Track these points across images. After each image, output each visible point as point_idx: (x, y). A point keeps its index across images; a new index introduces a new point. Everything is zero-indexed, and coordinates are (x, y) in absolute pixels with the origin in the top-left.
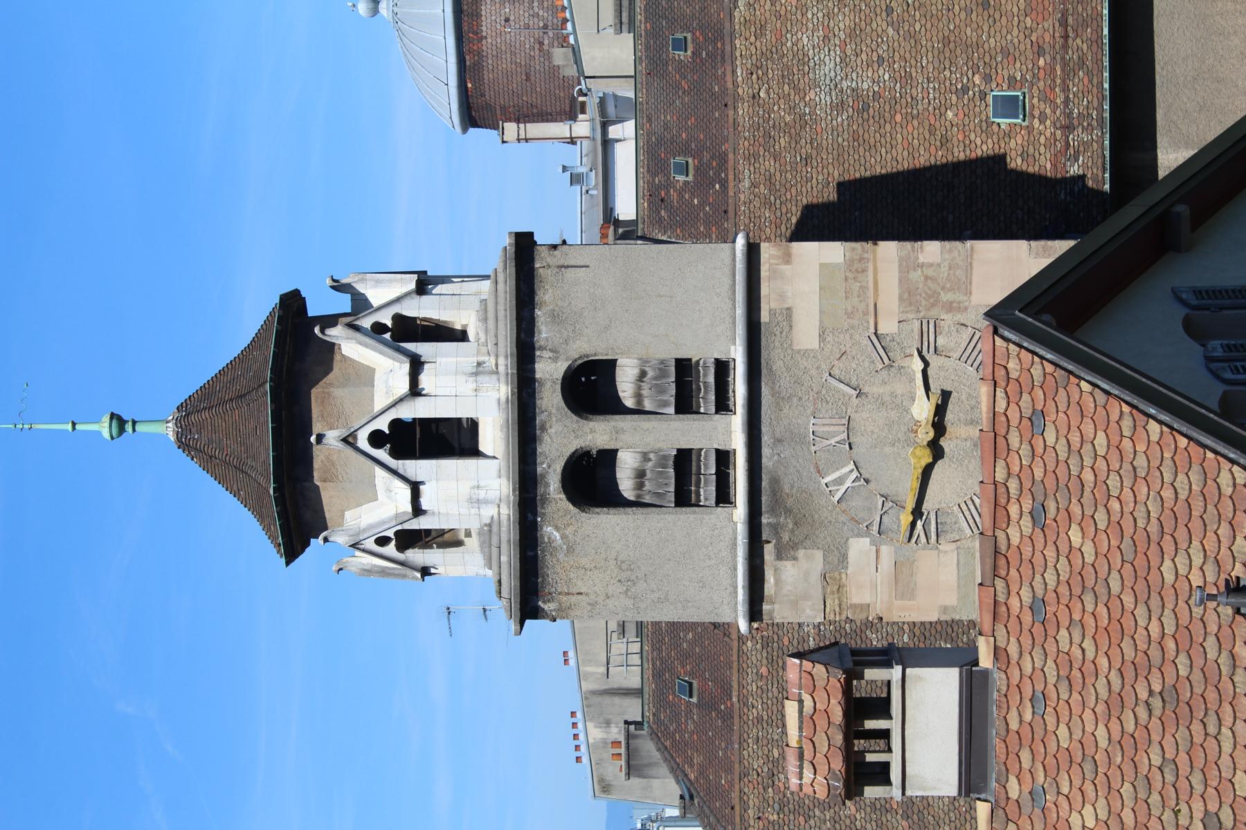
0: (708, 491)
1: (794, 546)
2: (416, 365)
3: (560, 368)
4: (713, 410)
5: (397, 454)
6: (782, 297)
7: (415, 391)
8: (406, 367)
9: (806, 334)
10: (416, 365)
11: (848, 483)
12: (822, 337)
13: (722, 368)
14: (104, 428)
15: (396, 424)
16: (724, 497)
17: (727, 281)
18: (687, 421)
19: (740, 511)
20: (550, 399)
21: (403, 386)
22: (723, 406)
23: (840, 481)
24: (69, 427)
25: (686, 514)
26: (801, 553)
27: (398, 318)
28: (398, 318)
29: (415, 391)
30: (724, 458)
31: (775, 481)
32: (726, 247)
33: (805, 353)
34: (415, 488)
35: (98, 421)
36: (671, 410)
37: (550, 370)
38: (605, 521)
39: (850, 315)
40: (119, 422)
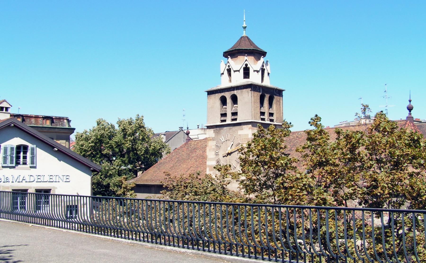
0: (223, 118)
1: (215, 133)
2: (239, 71)
3: (235, 94)
4: (232, 118)
5: (227, 70)
6: (245, 128)
7: (235, 71)
8: (238, 69)
9: (240, 132)
10: (239, 71)
11: (222, 140)
12: (240, 135)
13: (236, 119)
14: (245, 25)
15: (230, 69)
16: (222, 121)
17: (246, 119)
18: (230, 114)
19: (219, 123)
20: (232, 93)
21: (235, 70)
22: (233, 120)
23: (222, 139)
24: (244, 20)
25: (220, 116)
26: (214, 134)
27: (264, 69)
28: (264, 69)
29: (235, 71)
30: (225, 121)
31: (222, 129)
32: (251, 118)
33: (237, 132)
34: (223, 74)
35: (246, 24)
36: (232, 112)
37: (235, 92)
38: (218, 103)
39: (242, 139)
40: (245, 28)
